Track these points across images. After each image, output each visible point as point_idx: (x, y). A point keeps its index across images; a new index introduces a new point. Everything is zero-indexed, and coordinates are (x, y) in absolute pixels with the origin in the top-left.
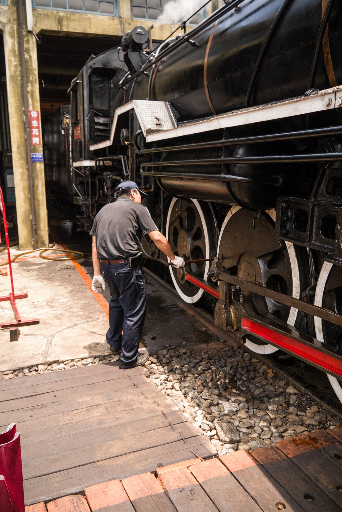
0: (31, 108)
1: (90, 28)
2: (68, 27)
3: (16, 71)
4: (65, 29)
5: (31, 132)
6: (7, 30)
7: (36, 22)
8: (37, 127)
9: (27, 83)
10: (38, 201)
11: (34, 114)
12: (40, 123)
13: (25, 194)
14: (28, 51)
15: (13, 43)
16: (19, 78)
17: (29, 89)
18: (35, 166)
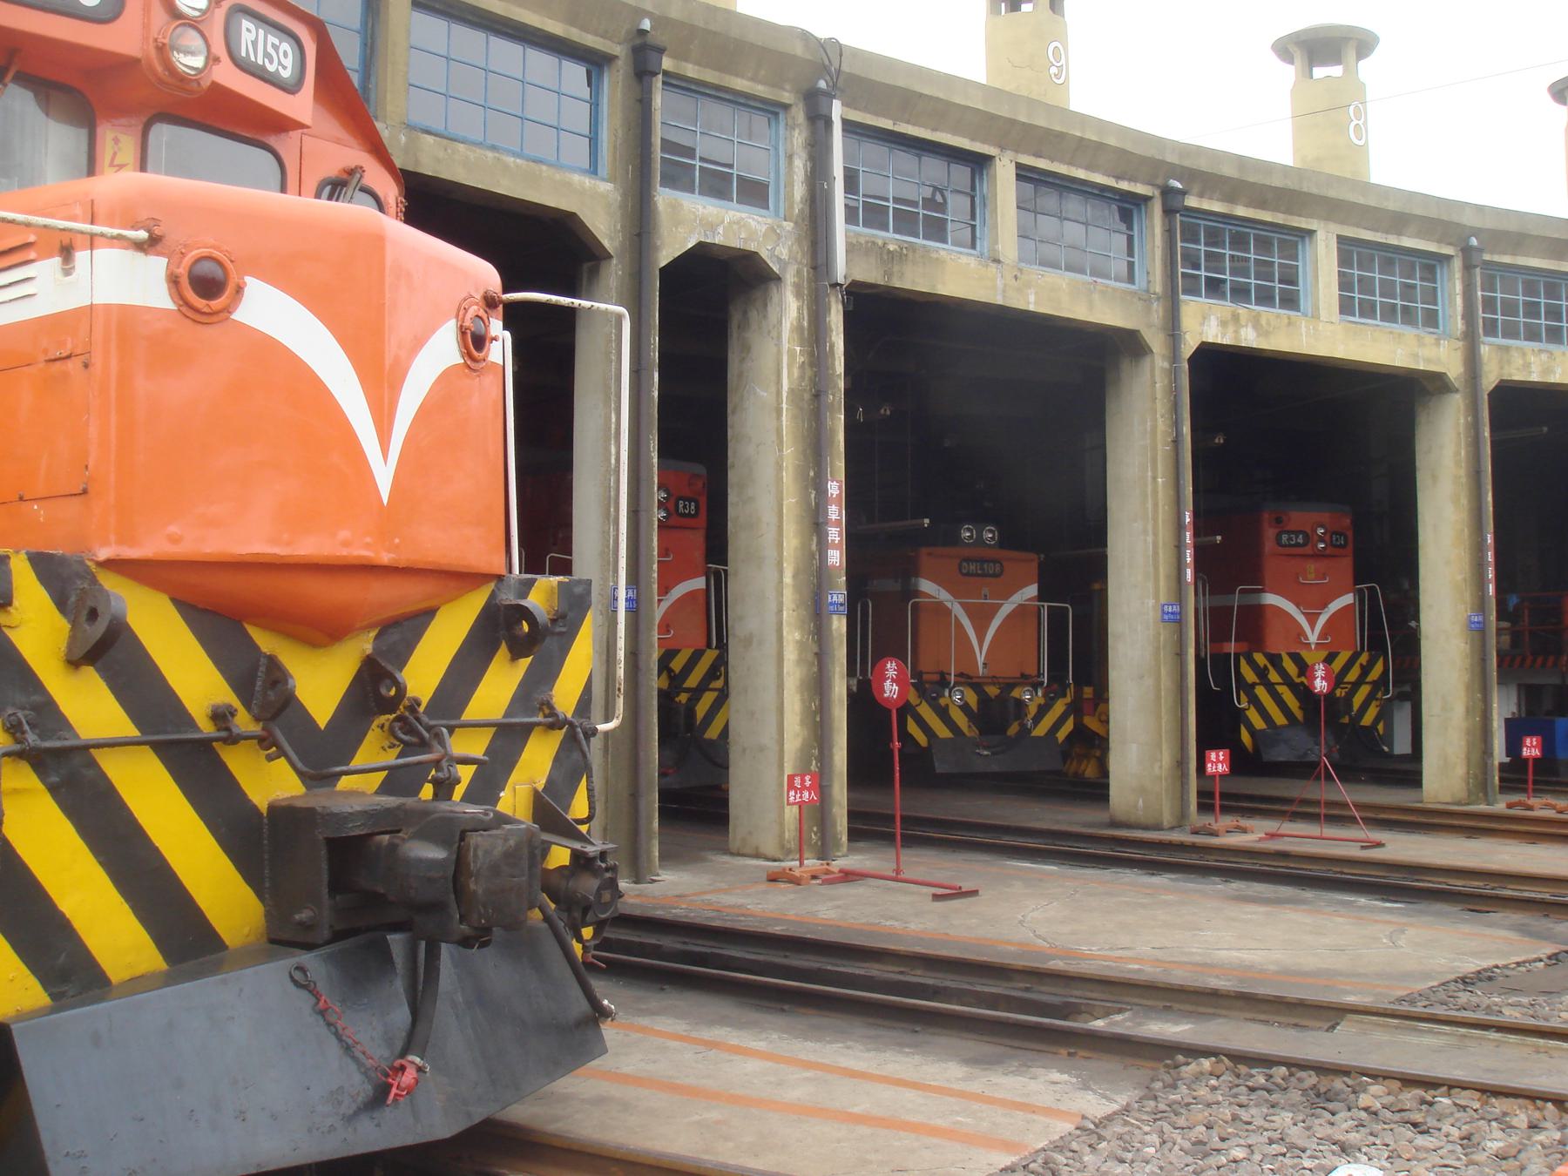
3: (802, 377)
6: (790, 278)
13: (803, 701)
16: (807, 396)
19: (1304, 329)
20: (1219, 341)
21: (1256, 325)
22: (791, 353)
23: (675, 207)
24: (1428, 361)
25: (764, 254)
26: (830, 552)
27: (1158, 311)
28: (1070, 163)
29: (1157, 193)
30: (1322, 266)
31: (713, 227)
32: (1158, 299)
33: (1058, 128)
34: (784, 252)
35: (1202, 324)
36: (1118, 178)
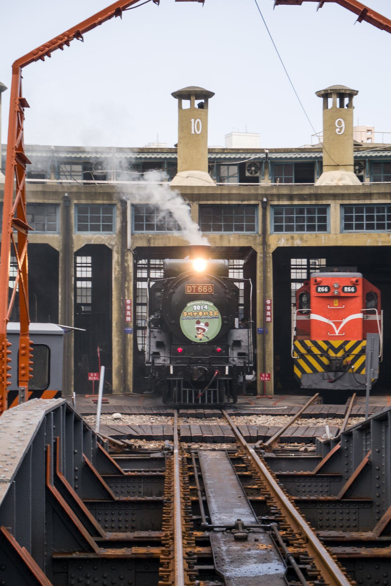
0: (126, 298)
1: (169, 243)
2: (154, 244)
3: (118, 274)
4: (152, 245)
5: (126, 313)
6: (115, 249)
7: (133, 242)
8: (130, 310)
9: (125, 282)
10: (128, 360)
11: (128, 302)
12: (132, 307)
14: (127, 261)
15: (118, 257)
17: (126, 285)
18: (127, 336)
19: (323, 238)
20: (285, 246)
21: (301, 239)
22: (115, 268)
23: (78, 237)
24: (384, 242)
25: (107, 244)
26: (127, 318)
27: (259, 240)
28: (221, 200)
29: (260, 203)
30: (335, 215)
31: (90, 240)
32: (259, 236)
33: (211, 192)
34: (113, 243)
35: (278, 241)
36: (243, 201)
